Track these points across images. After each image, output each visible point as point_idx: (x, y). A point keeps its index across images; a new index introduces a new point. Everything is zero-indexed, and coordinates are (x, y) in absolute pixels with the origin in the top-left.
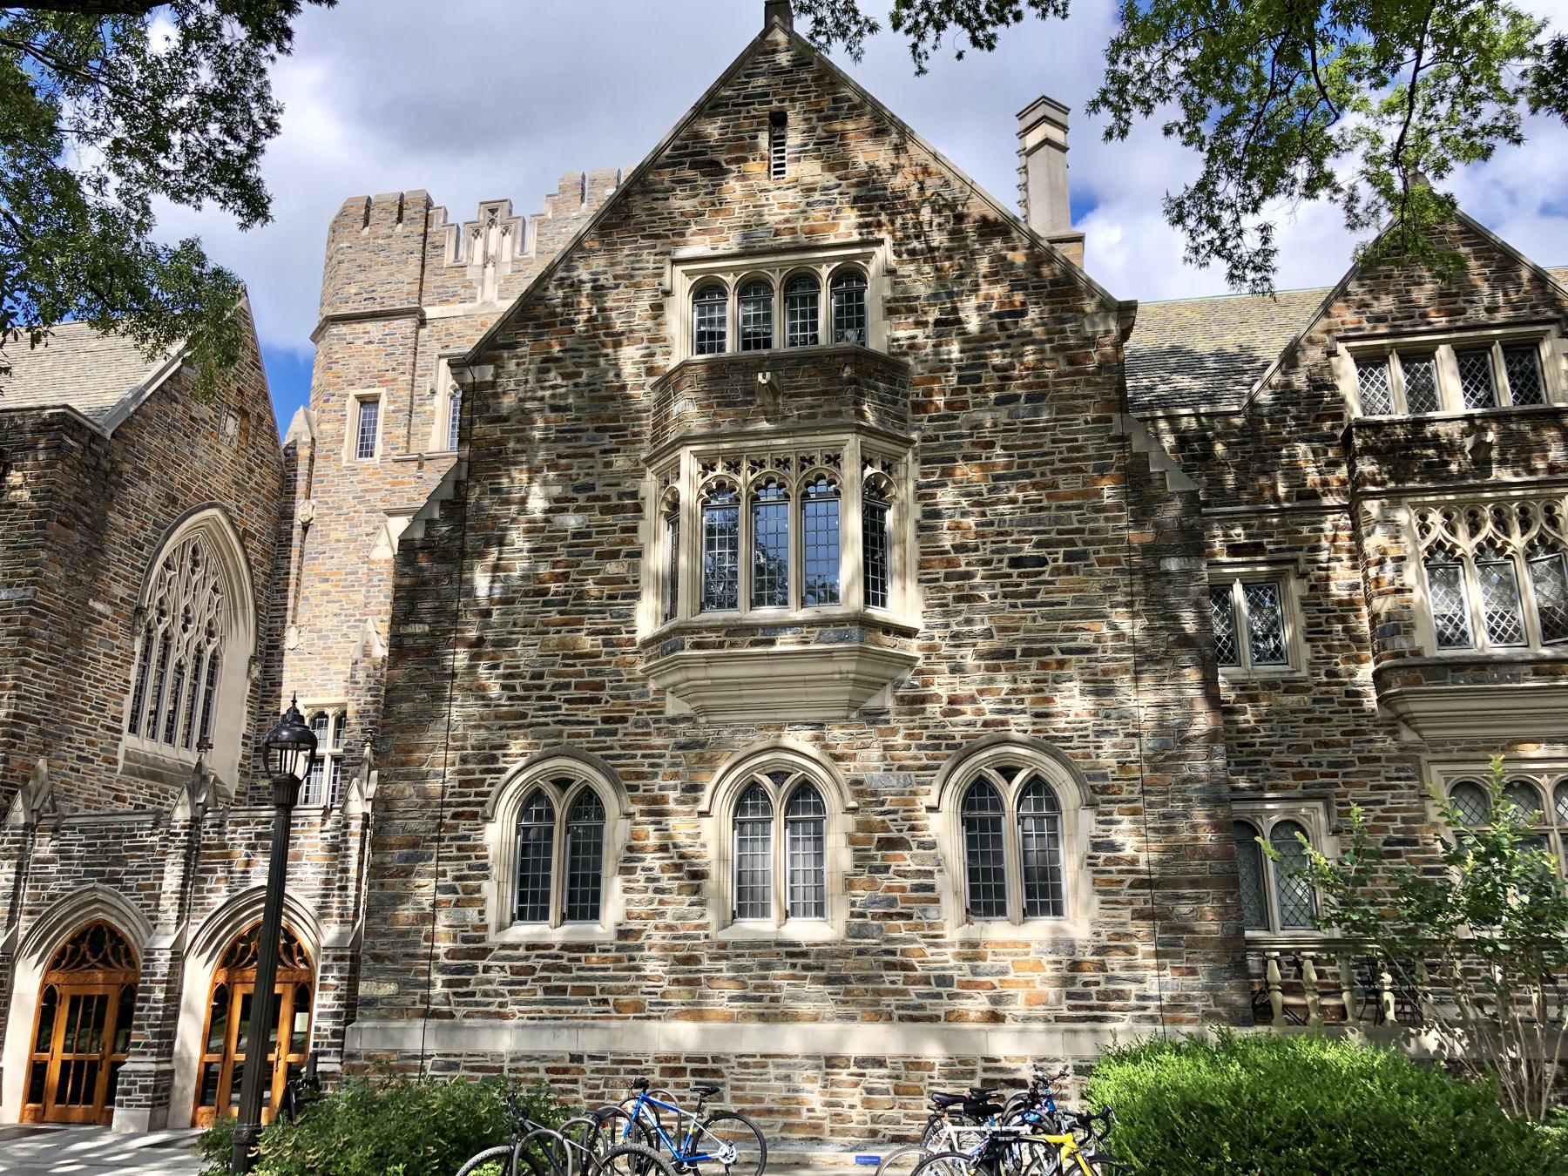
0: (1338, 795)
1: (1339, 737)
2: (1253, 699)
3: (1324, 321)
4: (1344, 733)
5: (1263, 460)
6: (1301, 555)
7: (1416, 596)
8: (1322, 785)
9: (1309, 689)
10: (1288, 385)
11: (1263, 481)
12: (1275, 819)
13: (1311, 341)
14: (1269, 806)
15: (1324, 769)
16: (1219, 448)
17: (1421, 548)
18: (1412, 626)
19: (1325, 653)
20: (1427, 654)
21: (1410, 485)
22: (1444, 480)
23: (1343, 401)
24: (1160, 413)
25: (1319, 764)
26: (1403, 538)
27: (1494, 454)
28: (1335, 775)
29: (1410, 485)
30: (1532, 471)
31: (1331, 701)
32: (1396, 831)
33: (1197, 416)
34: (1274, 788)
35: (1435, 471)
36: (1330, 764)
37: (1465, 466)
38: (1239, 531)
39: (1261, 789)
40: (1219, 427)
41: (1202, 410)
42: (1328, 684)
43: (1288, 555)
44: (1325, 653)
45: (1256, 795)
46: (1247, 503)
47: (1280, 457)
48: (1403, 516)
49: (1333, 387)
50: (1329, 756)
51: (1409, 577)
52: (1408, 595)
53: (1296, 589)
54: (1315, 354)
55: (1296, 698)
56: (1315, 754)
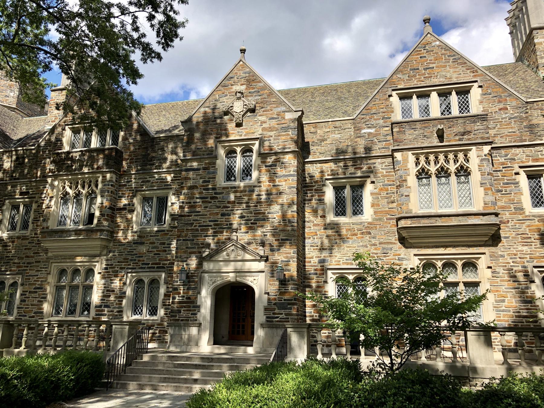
0: (27, 273)
1: (32, 255)
2: (13, 242)
3: (65, 119)
4: (34, 253)
5: (36, 165)
6: (37, 196)
7: (52, 209)
8: (24, 270)
9: (28, 239)
10: (49, 140)
11: (35, 171)
12: (12, 281)
13: (59, 125)
14: (8, 277)
15: (26, 265)
16: (26, 160)
17: (60, 193)
18: (49, 219)
19: (36, 227)
20: (50, 228)
21: (61, 173)
22: (70, 171)
23: (62, 145)
24: (13, 149)
25: (24, 263)
26: (55, 191)
27: (85, 163)
28: (28, 267)
29: (61, 173)
30: (93, 169)
31: (33, 243)
32: (38, 285)
33: (23, 150)
34: (10, 271)
35: (69, 169)
36: (28, 263)
37: (77, 167)
38: (24, 188)
39: (7, 271)
40: (28, 153)
41: (24, 148)
42: (34, 237)
43: (33, 196)
44: (36, 227)
45: (4, 273)
46: (29, 178)
47: (41, 163)
48: (56, 183)
49: (62, 141)
50: (26, 260)
51: (53, 203)
52: (50, 209)
53: (34, 206)
54: (59, 129)
55: (24, 241)
56: (24, 261)
